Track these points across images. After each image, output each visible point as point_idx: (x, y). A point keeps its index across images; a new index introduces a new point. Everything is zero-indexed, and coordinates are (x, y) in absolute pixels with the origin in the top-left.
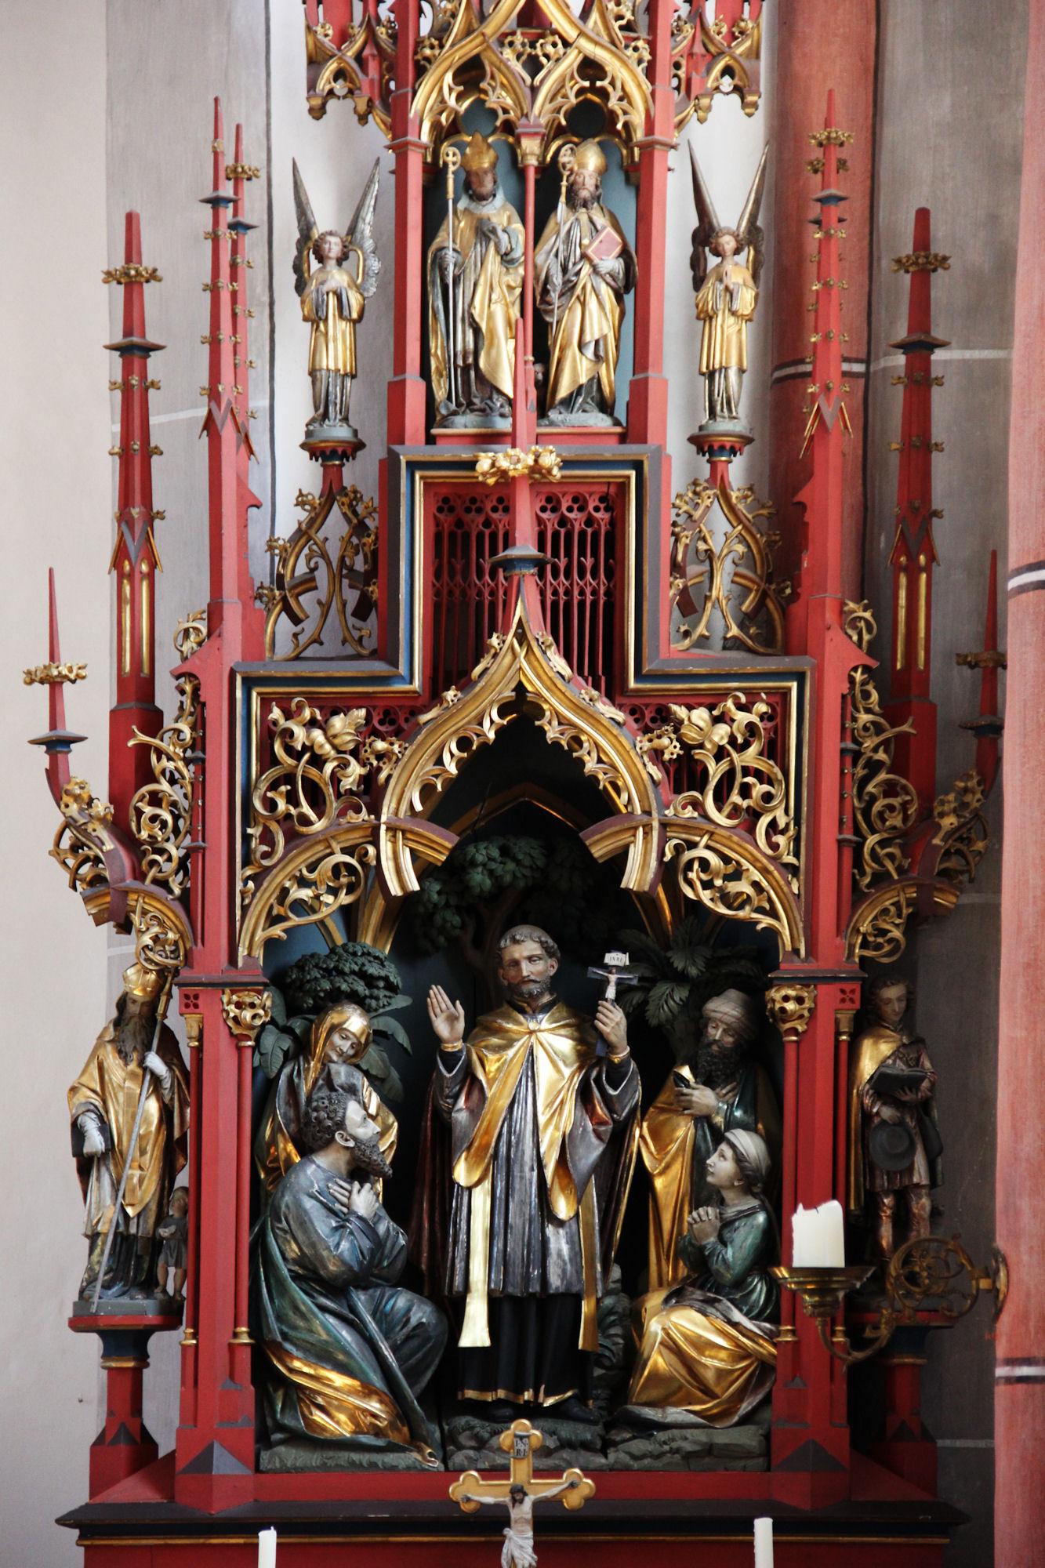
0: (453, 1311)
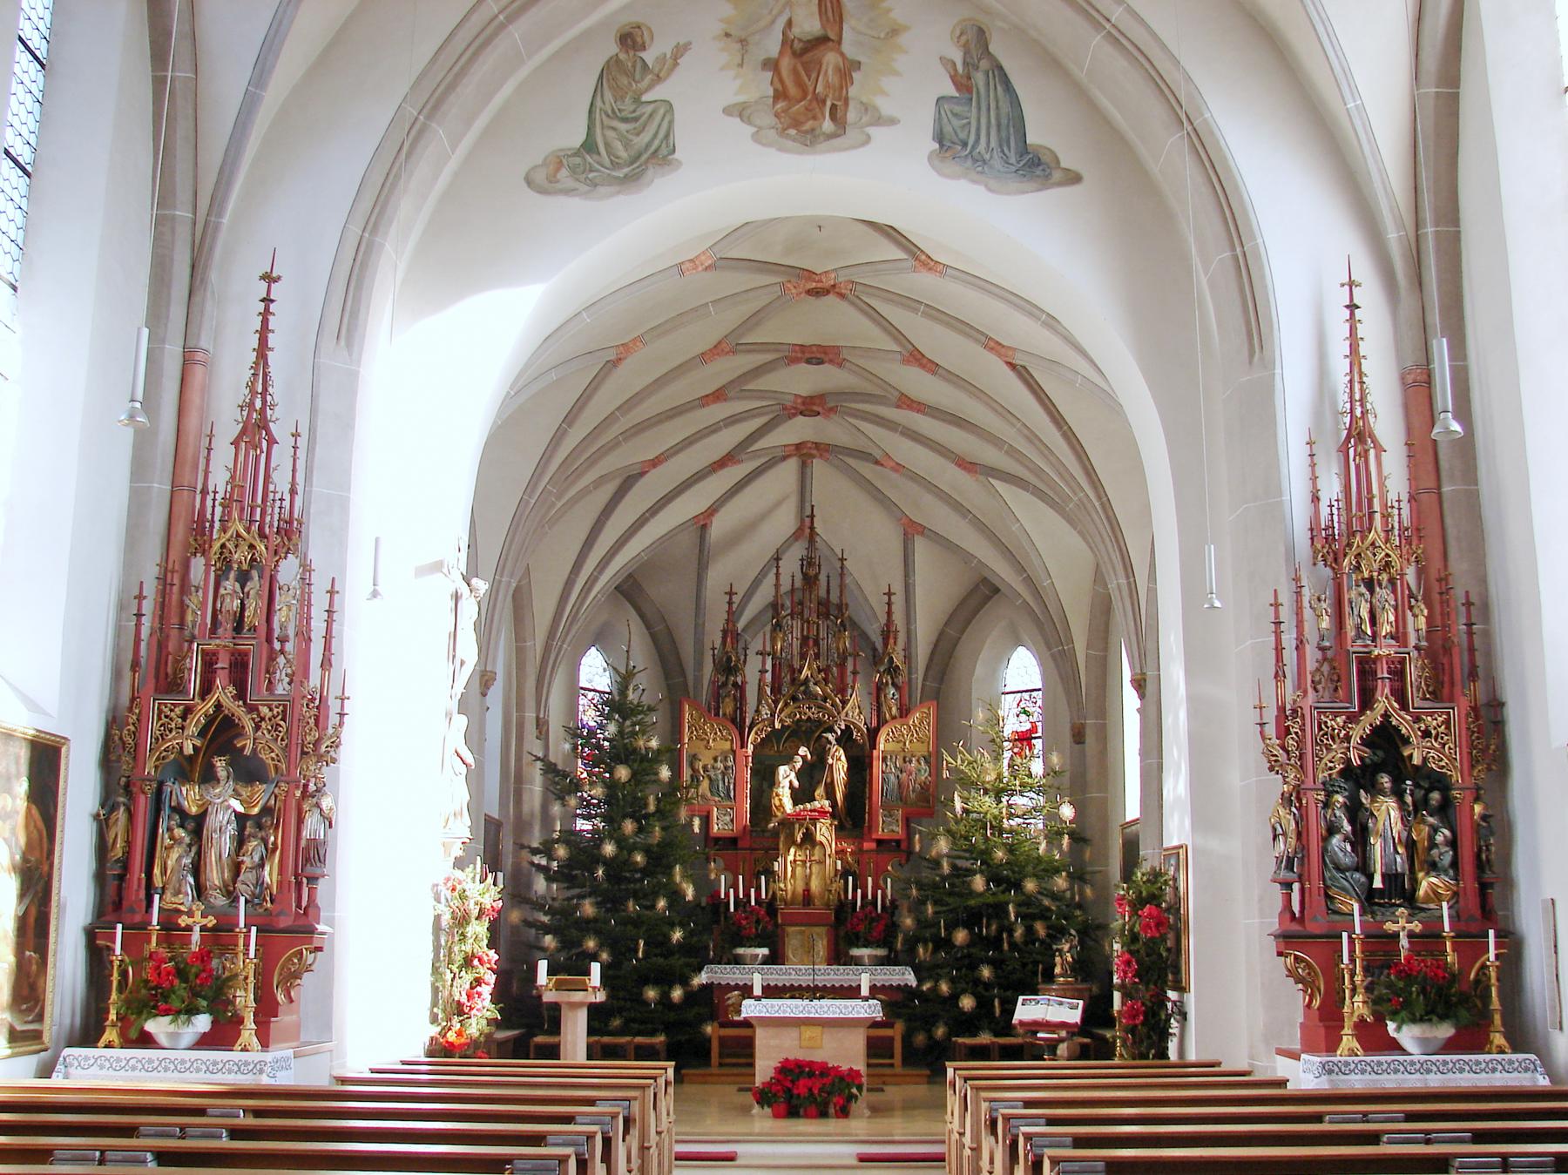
0: (1370, 877)
